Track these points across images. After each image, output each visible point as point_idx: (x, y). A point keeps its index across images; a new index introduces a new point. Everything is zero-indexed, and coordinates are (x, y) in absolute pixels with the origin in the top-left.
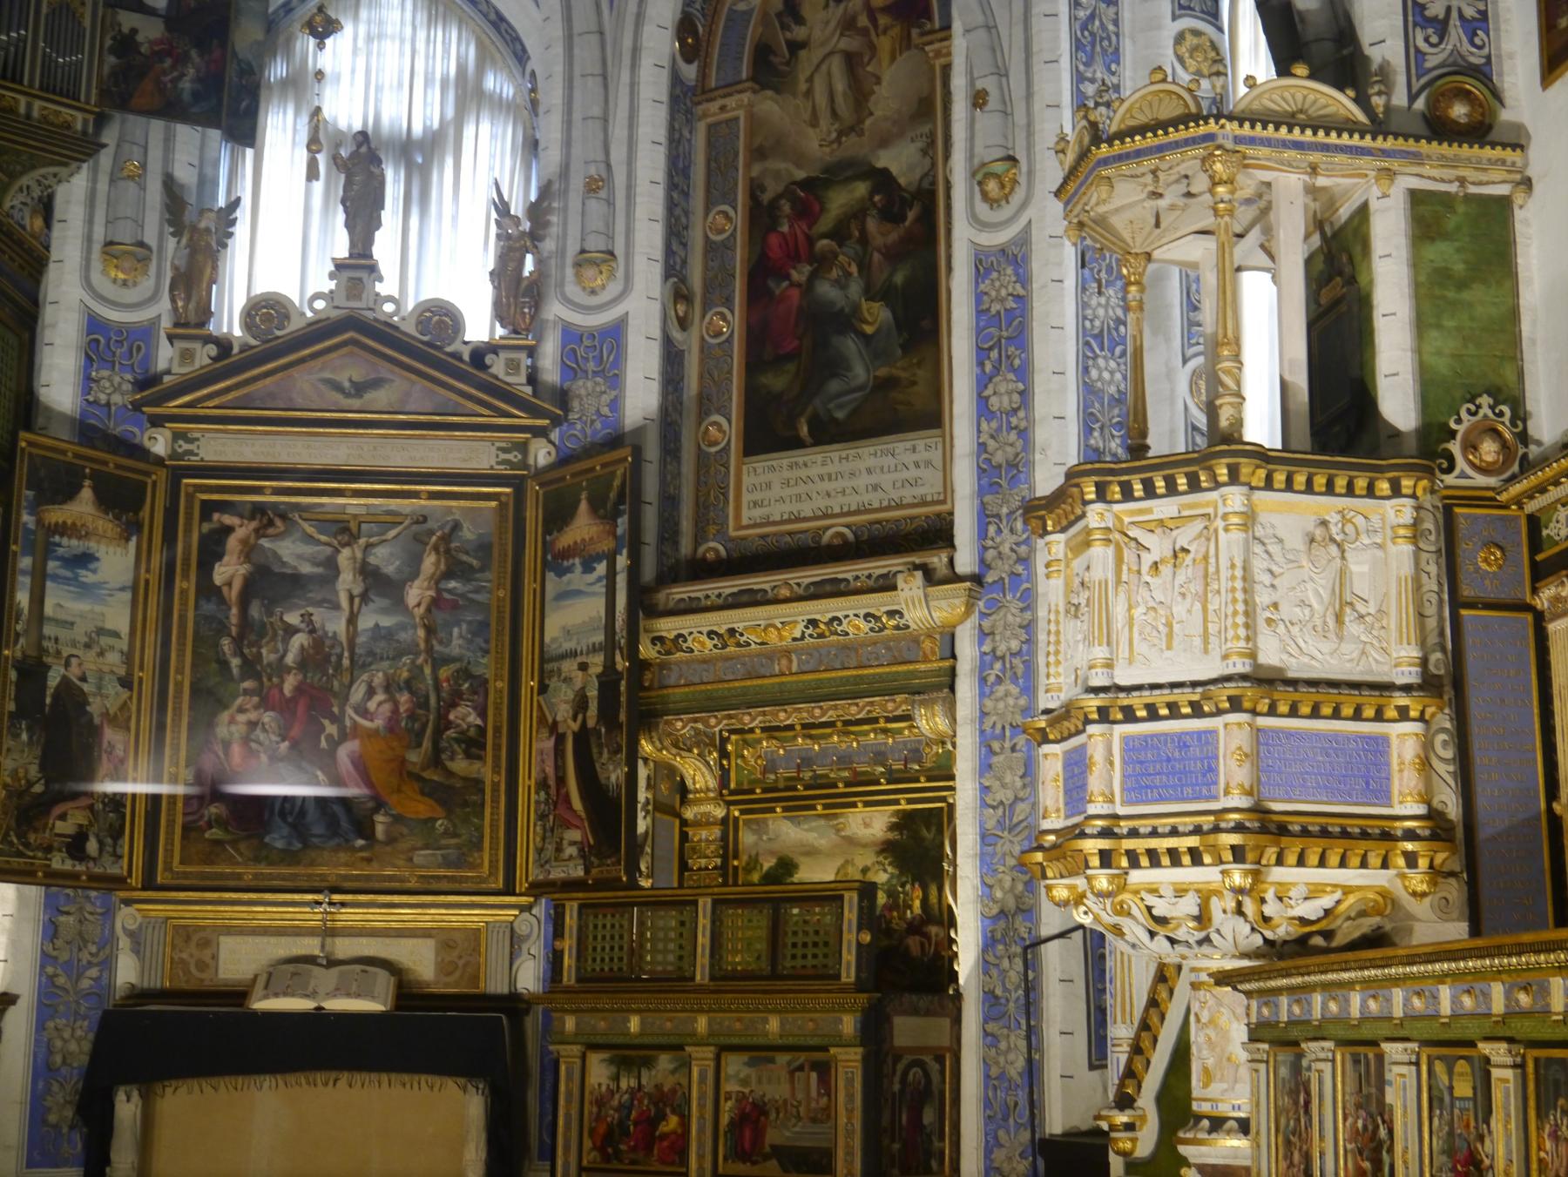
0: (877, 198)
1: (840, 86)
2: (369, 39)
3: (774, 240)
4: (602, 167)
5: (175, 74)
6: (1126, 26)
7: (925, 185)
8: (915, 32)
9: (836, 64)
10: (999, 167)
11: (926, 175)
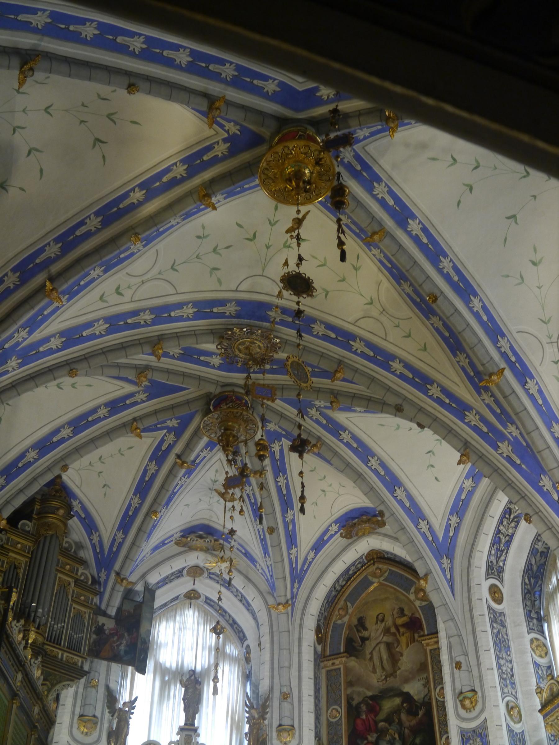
0: (405, 705)
1: (385, 656)
2: (180, 629)
3: (359, 722)
4: (289, 688)
5: (118, 643)
6: (510, 637)
7: (426, 699)
8: (416, 636)
9: (383, 647)
10: (470, 694)
11: (426, 695)
